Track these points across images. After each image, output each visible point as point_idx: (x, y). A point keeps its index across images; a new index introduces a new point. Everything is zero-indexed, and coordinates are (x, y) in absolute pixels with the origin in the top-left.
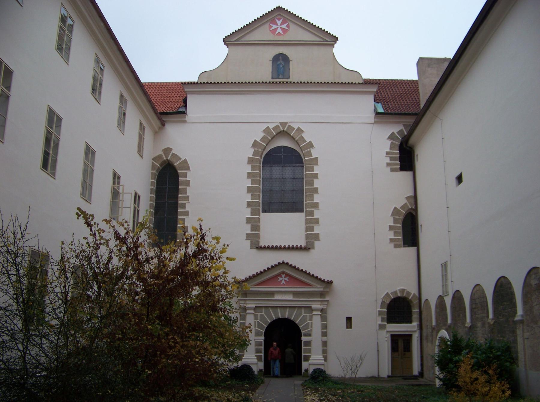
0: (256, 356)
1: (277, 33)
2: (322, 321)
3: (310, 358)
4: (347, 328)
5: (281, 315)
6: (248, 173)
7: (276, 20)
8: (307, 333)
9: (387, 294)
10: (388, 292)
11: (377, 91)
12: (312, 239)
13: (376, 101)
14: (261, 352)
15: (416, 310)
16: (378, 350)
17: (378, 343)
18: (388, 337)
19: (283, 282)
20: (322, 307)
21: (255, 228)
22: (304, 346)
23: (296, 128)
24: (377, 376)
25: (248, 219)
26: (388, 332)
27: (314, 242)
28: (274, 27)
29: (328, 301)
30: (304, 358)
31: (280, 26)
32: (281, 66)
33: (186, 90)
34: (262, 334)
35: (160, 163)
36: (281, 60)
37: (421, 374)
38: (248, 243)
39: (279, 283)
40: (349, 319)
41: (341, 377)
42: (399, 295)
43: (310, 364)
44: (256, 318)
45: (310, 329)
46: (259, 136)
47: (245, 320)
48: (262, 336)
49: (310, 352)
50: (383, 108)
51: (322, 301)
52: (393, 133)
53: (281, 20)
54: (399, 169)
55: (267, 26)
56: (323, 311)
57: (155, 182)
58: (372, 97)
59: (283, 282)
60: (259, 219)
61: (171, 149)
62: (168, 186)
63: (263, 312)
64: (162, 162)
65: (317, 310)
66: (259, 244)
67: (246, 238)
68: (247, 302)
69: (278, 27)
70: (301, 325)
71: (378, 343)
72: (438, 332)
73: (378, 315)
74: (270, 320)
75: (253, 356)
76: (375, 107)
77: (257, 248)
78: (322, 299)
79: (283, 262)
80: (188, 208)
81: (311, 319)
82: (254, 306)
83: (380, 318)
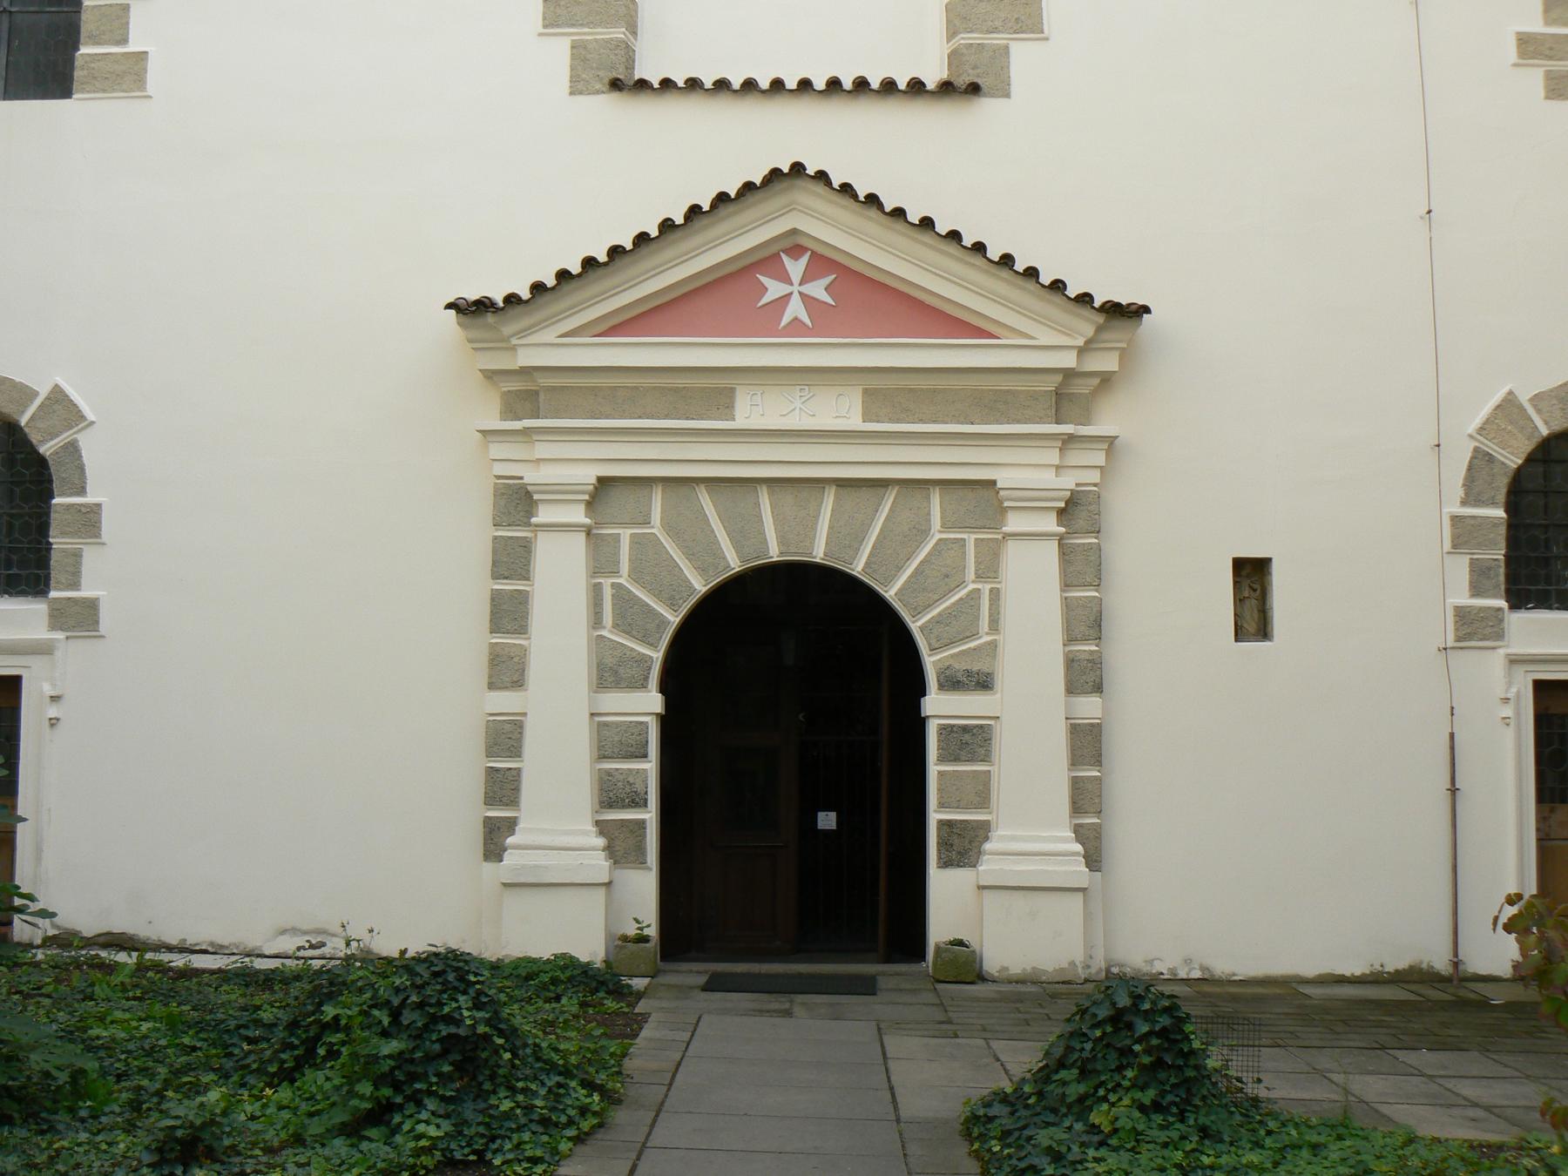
0: (602, 827)
2: (1066, 585)
3: (987, 846)
4: (1240, 635)
5: (782, 540)
8: (960, 666)
9: (1509, 405)
10: (1511, 393)
12: (995, 30)
14: (638, 802)
16: (1454, 791)
17: (1452, 736)
18: (1518, 695)
19: (796, 309)
20: (1068, 482)
22: (942, 759)
24: (1441, 964)
26: (1514, 661)
27: (1006, 49)
29: (1110, 442)
30: (944, 844)
34: (646, 678)
38: (558, 52)
39: (767, 320)
41: (1196, 974)
43: (981, 888)
44: (601, 556)
45: (989, 638)
47: (526, 576)
48: (643, 686)
49: (983, 798)
51: (1068, 441)
56: (1072, 508)
59: (796, 309)
63: (656, 516)
65: (1031, 501)
66: (630, 64)
67: (540, 22)
68: (542, 450)
70: (916, 614)
71: (1452, 736)
73: (1447, 546)
74: (702, 570)
75: (585, 833)
77: (616, 85)
78: (1068, 429)
79: (798, 168)
81: (989, 568)
82: (588, 475)
83: (1460, 569)
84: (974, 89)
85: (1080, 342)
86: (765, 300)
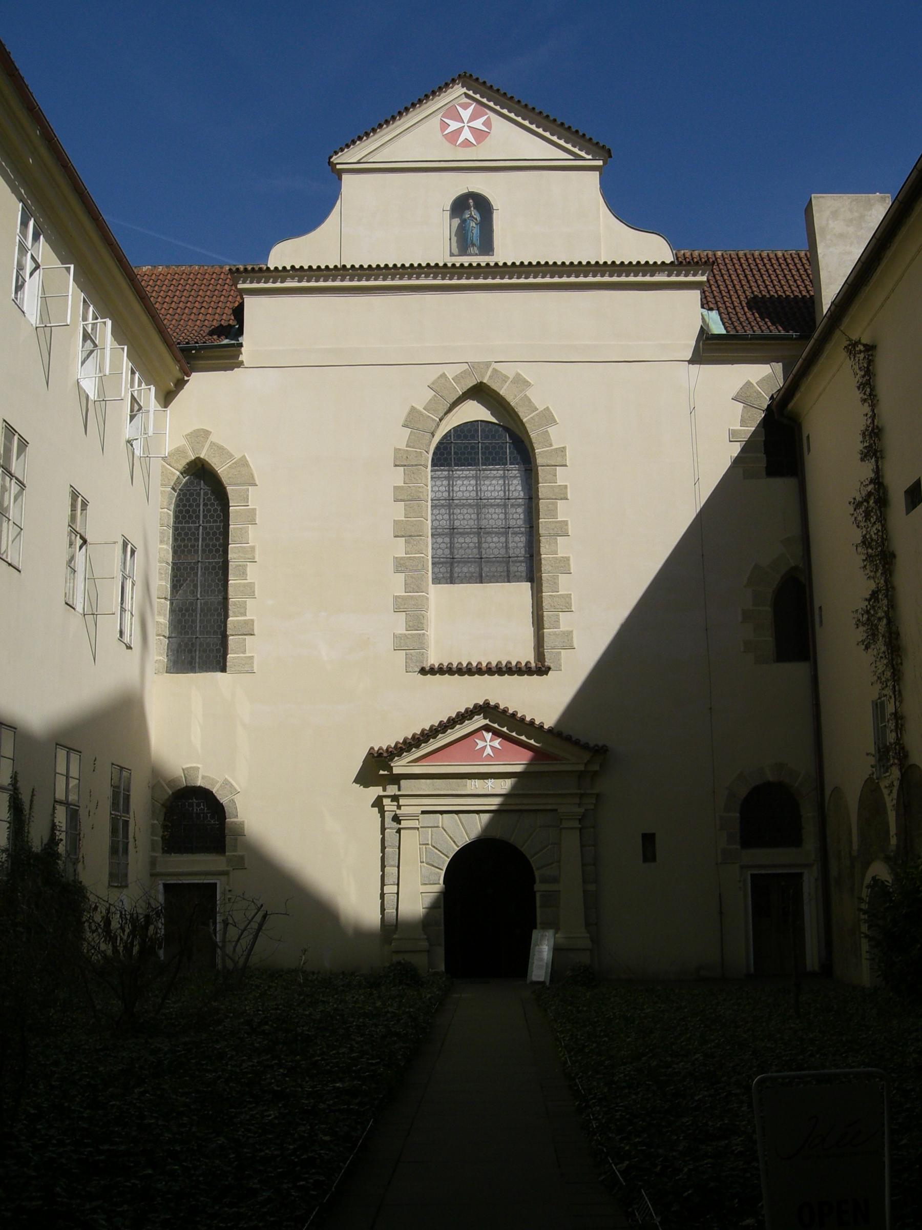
4: (646, 859)
6: (396, 488)
7: (458, 107)
11: (708, 280)
13: (705, 306)
15: (808, 813)
17: (720, 894)
19: (488, 751)
21: (417, 622)
23: (511, 376)
25: (400, 600)
28: (454, 125)
29: (598, 796)
31: (467, 123)
32: (473, 224)
33: (240, 286)
35: (181, 467)
36: (472, 209)
37: (827, 969)
40: (649, 839)
42: (770, 777)
46: (421, 398)
50: (724, 324)
52: (749, 384)
54: (764, 473)
55: (435, 121)
57: (171, 513)
58: (695, 296)
59: (488, 751)
60: (427, 599)
61: (207, 433)
62: (203, 523)
64: (188, 464)
69: (463, 125)
72: (866, 865)
76: (703, 319)
80: (253, 573)
84: (549, 669)
85: (585, 761)
86: (478, 748)
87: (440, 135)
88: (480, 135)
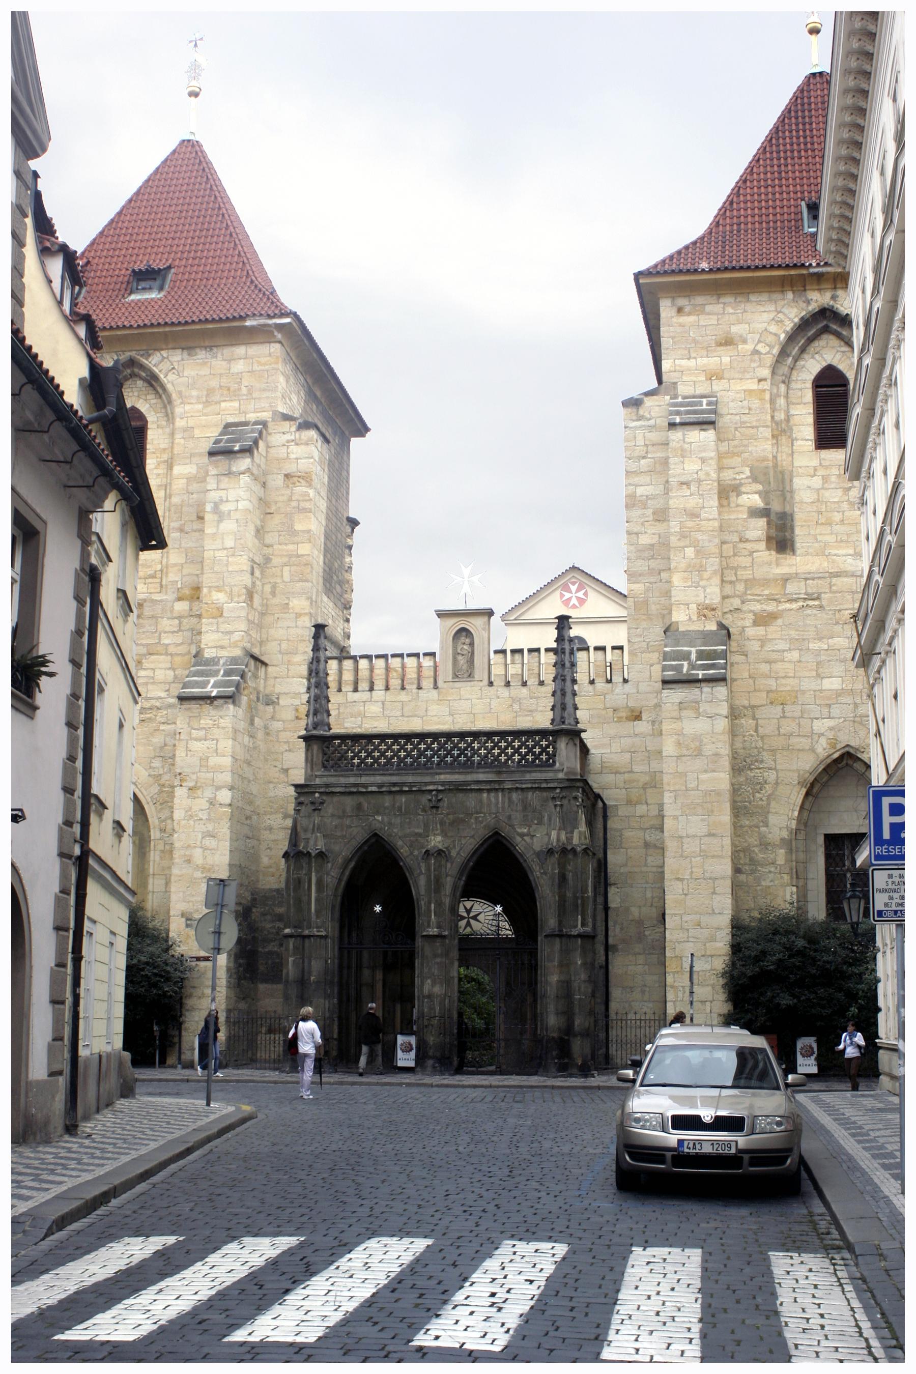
1: (571, 604)
28: (567, 595)
53: (577, 585)
55: (558, 593)
87: (559, 602)
88: (582, 601)
